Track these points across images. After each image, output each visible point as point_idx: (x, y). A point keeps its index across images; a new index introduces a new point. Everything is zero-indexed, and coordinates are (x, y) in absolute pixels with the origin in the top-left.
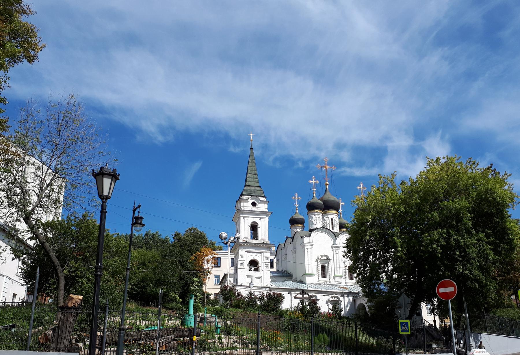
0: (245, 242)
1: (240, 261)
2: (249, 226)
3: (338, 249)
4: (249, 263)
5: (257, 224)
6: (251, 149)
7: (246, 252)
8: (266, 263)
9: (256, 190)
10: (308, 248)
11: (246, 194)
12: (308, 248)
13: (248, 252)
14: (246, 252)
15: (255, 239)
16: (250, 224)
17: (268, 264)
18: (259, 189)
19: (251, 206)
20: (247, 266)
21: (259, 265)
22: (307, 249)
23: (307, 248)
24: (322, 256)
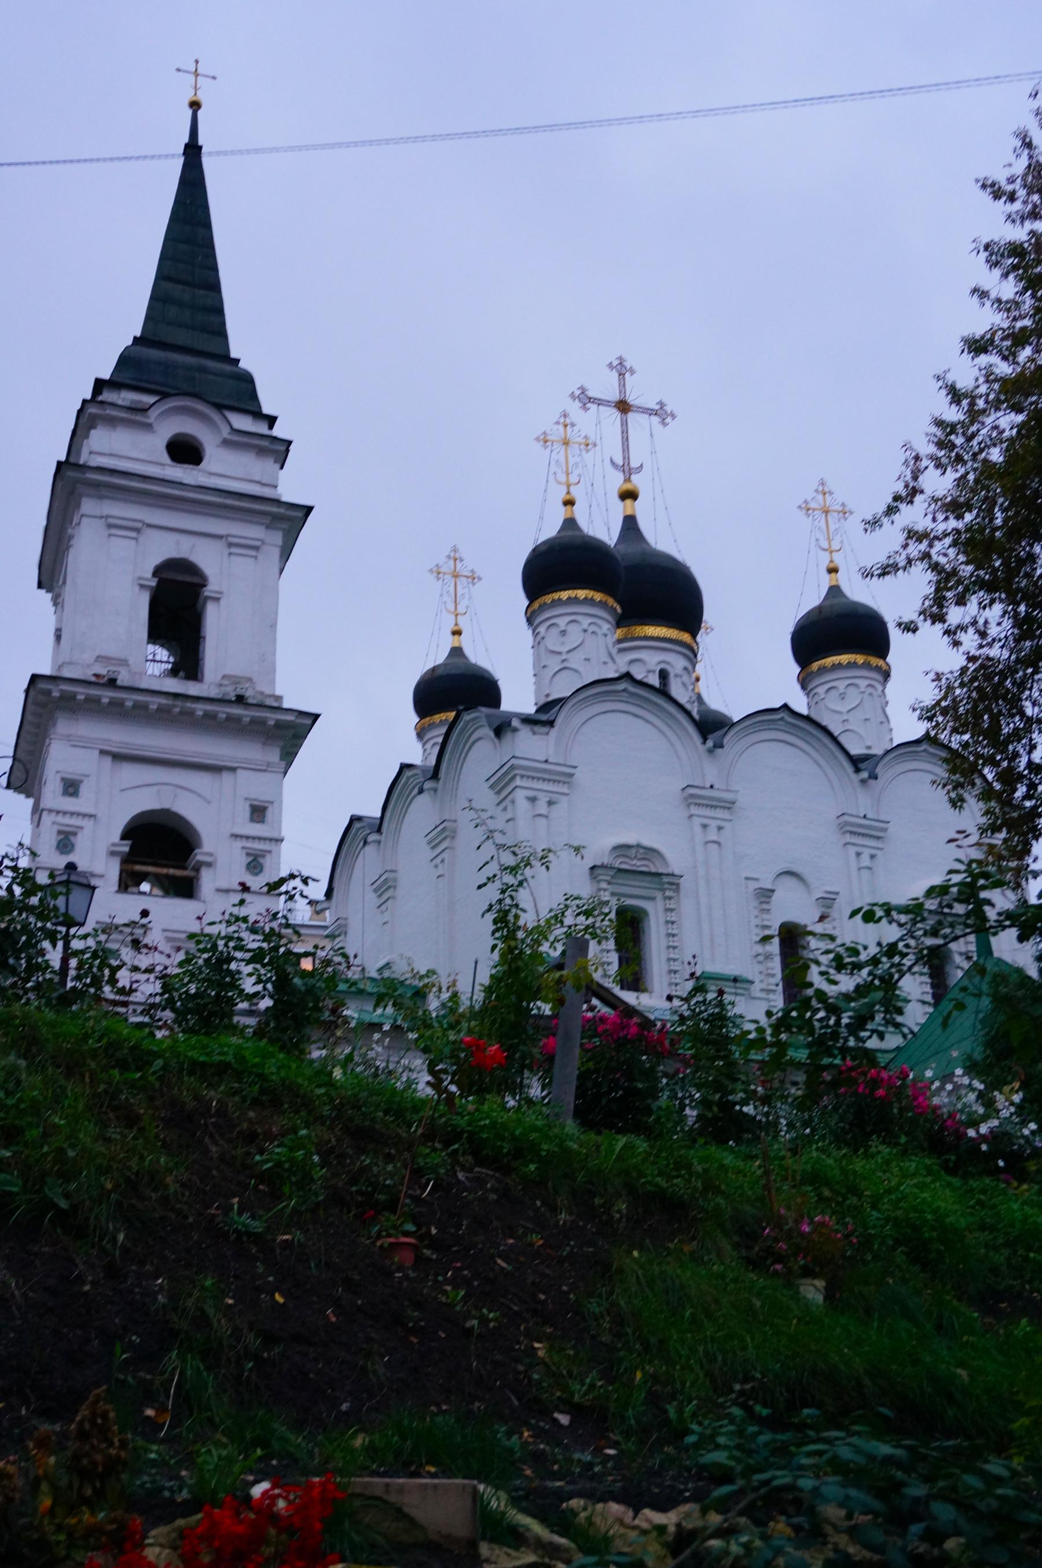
0: (102, 681)
1: (53, 816)
2: (142, 586)
3: (719, 813)
4: (124, 837)
5: (196, 580)
6: (187, 146)
7: (103, 752)
8: (249, 844)
9: (203, 370)
10: (540, 795)
11: (133, 383)
12: (540, 795)
13: (118, 757)
14: (103, 752)
15: (182, 674)
16: (149, 574)
17: (263, 854)
18: (228, 368)
19: (166, 458)
20: (113, 854)
21: (199, 856)
22: (533, 800)
23: (531, 794)
24: (622, 849)
